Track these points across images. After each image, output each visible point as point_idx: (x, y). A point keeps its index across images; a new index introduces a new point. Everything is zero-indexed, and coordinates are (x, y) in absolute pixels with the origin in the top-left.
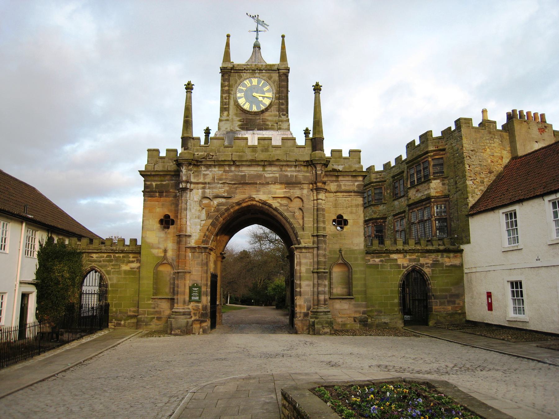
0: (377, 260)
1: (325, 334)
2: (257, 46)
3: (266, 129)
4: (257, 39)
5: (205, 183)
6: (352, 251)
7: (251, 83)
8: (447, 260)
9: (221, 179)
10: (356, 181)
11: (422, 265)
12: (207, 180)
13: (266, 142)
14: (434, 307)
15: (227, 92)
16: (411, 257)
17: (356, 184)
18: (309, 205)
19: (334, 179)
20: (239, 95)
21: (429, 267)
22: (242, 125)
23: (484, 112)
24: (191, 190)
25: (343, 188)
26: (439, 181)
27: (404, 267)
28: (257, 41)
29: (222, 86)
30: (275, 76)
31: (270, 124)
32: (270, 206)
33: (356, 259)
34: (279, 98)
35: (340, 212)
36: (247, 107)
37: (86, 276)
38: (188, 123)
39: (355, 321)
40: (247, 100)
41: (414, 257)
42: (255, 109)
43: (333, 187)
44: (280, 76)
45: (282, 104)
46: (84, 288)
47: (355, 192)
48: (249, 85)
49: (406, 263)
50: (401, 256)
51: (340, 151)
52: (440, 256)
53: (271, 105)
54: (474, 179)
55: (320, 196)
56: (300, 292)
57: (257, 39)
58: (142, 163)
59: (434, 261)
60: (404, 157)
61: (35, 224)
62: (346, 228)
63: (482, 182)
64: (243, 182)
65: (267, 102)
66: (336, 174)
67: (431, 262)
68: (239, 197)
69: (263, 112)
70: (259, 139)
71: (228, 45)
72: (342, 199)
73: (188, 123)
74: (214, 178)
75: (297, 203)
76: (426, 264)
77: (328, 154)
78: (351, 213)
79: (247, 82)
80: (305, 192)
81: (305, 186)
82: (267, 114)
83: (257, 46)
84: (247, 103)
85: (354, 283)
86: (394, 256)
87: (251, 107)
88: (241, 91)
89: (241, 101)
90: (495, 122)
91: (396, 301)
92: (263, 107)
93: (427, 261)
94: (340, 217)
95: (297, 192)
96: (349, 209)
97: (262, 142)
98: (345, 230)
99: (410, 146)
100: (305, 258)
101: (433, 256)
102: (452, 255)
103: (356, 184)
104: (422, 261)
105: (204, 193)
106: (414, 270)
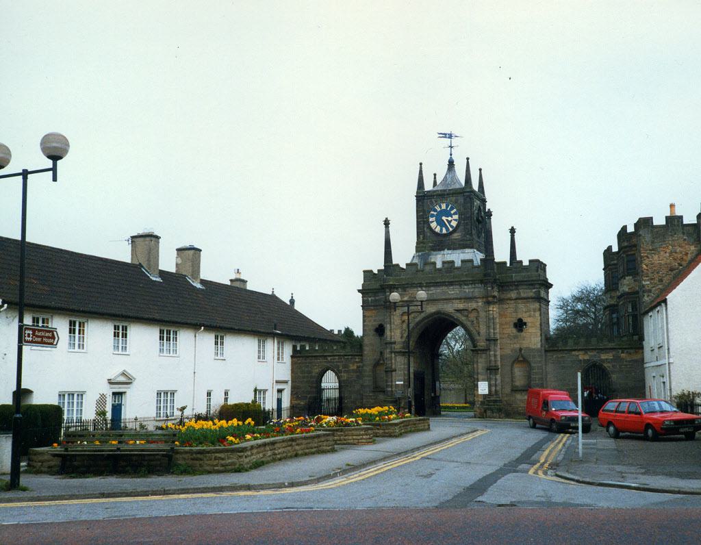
2: (451, 164)
4: (451, 155)
7: (441, 207)
10: (534, 289)
11: (603, 361)
13: (451, 265)
17: (534, 290)
18: (482, 314)
20: (431, 219)
21: (609, 362)
23: (672, 206)
25: (523, 295)
26: (631, 277)
28: (451, 158)
30: (461, 199)
33: (534, 357)
35: (520, 316)
36: (438, 230)
37: (323, 375)
40: (438, 224)
42: (444, 231)
43: (513, 295)
44: (465, 199)
46: (323, 385)
47: (532, 298)
48: (439, 209)
49: (586, 357)
54: (652, 279)
55: (491, 309)
57: (451, 155)
58: (359, 282)
60: (615, 249)
61: (283, 337)
63: (661, 280)
66: (517, 285)
69: (451, 233)
70: (444, 263)
72: (521, 306)
75: (472, 316)
78: (530, 316)
80: (480, 304)
83: (451, 164)
84: (438, 227)
87: (441, 230)
88: (432, 216)
89: (433, 225)
90: (681, 217)
94: (520, 320)
95: (473, 305)
96: (528, 313)
97: (446, 265)
99: (623, 234)
100: (481, 357)
102: (632, 351)
104: (604, 357)
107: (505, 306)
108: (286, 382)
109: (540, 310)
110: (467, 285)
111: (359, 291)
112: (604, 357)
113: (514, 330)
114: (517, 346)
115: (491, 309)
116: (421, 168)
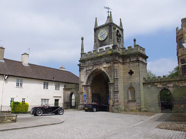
0: (149, 86)
1: (115, 112)
3: (106, 45)
5: (86, 66)
6: (135, 83)
8: (181, 84)
9: (90, 64)
10: (136, 57)
11: (168, 87)
12: (87, 65)
14: (174, 106)
15: (96, 36)
16: (163, 84)
17: (136, 58)
19: (129, 57)
21: (171, 88)
22: (100, 46)
24: (83, 69)
25: (132, 60)
27: (160, 88)
29: (95, 34)
30: (108, 27)
31: (107, 43)
32: (102, 70)
33: (137, 86)
34: (109, 34)
38: (82, 49)
39: (137, 109)
41: (165, 84)
42: (103, 40)
45: (111, 35)
46: (72, 98)
47: (135, 61)
49: (161, 86)
50: (159, 84)
51: (130, 47)
52: (177, 82)
53: (107, 37)
56: (111, 98)
59: (174, 85)
62: (133, 75)
64: (95, 65)
65: (106, 36)
67: (173, 85)
68: (94, 69)
69: (105, 40)
71: (96, 21)
72: (131, 65)
73: (82, 49)
74: (88, 64)
76: (170, 86)
77: (127, 49)
79: (100, 32)
81: (112, 63)
82: (107, 40)
85: (136, 94)
86: (156, 84)
91: (157, 102)
92: (105, 38)
93: (171, 85)
94: (131, 71)
98: (132, 75)
101: (174, 83)
102: (183, 82)
103: (136, 58)
104: (168, 85)
105: (86, 69)
106: (165, 89)
107: (125, 65)
108: (61, 97)
109: (139, 65)
110: (107, 57)
111: (78, 65)
112: (168, 85)
113: (129, 75)
114: (130, 82)
115: (115, 65)
116: (96, 20)
